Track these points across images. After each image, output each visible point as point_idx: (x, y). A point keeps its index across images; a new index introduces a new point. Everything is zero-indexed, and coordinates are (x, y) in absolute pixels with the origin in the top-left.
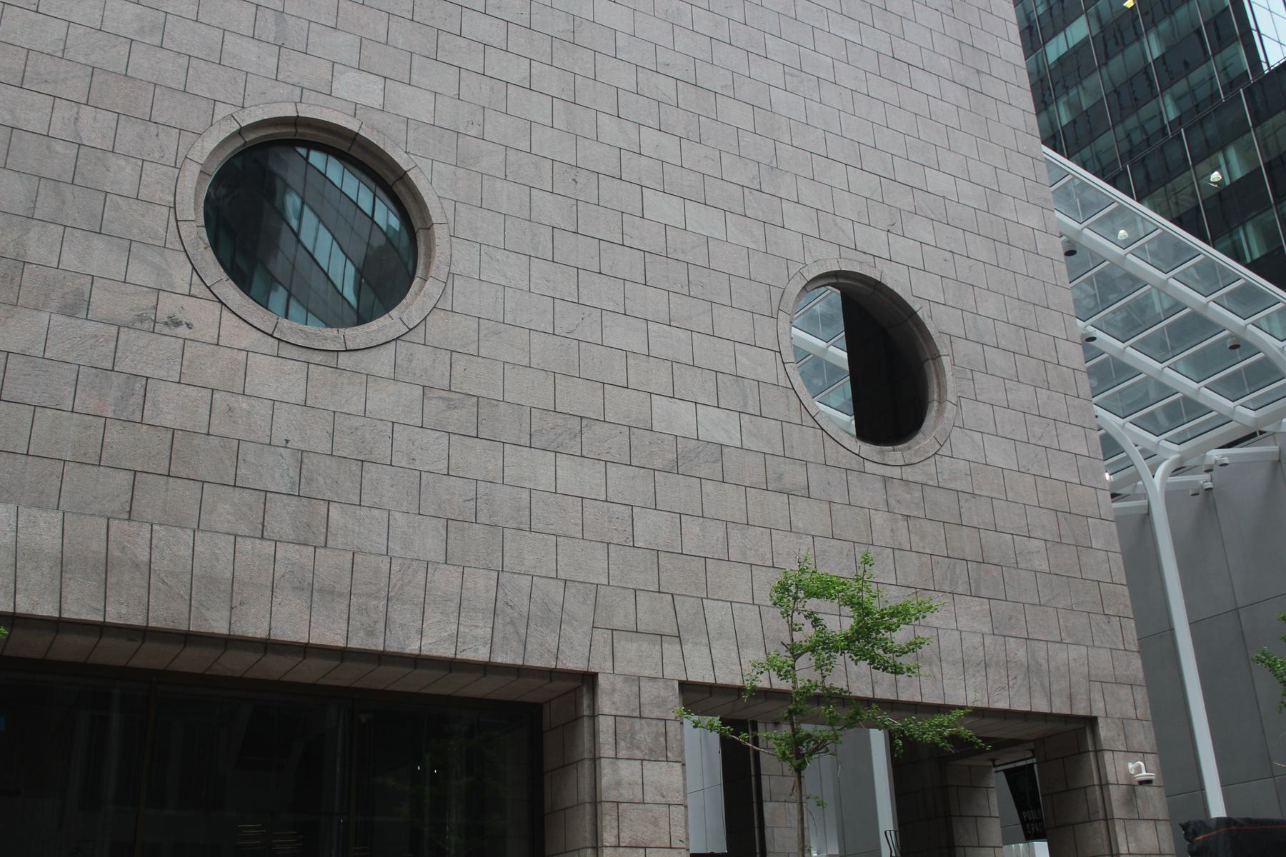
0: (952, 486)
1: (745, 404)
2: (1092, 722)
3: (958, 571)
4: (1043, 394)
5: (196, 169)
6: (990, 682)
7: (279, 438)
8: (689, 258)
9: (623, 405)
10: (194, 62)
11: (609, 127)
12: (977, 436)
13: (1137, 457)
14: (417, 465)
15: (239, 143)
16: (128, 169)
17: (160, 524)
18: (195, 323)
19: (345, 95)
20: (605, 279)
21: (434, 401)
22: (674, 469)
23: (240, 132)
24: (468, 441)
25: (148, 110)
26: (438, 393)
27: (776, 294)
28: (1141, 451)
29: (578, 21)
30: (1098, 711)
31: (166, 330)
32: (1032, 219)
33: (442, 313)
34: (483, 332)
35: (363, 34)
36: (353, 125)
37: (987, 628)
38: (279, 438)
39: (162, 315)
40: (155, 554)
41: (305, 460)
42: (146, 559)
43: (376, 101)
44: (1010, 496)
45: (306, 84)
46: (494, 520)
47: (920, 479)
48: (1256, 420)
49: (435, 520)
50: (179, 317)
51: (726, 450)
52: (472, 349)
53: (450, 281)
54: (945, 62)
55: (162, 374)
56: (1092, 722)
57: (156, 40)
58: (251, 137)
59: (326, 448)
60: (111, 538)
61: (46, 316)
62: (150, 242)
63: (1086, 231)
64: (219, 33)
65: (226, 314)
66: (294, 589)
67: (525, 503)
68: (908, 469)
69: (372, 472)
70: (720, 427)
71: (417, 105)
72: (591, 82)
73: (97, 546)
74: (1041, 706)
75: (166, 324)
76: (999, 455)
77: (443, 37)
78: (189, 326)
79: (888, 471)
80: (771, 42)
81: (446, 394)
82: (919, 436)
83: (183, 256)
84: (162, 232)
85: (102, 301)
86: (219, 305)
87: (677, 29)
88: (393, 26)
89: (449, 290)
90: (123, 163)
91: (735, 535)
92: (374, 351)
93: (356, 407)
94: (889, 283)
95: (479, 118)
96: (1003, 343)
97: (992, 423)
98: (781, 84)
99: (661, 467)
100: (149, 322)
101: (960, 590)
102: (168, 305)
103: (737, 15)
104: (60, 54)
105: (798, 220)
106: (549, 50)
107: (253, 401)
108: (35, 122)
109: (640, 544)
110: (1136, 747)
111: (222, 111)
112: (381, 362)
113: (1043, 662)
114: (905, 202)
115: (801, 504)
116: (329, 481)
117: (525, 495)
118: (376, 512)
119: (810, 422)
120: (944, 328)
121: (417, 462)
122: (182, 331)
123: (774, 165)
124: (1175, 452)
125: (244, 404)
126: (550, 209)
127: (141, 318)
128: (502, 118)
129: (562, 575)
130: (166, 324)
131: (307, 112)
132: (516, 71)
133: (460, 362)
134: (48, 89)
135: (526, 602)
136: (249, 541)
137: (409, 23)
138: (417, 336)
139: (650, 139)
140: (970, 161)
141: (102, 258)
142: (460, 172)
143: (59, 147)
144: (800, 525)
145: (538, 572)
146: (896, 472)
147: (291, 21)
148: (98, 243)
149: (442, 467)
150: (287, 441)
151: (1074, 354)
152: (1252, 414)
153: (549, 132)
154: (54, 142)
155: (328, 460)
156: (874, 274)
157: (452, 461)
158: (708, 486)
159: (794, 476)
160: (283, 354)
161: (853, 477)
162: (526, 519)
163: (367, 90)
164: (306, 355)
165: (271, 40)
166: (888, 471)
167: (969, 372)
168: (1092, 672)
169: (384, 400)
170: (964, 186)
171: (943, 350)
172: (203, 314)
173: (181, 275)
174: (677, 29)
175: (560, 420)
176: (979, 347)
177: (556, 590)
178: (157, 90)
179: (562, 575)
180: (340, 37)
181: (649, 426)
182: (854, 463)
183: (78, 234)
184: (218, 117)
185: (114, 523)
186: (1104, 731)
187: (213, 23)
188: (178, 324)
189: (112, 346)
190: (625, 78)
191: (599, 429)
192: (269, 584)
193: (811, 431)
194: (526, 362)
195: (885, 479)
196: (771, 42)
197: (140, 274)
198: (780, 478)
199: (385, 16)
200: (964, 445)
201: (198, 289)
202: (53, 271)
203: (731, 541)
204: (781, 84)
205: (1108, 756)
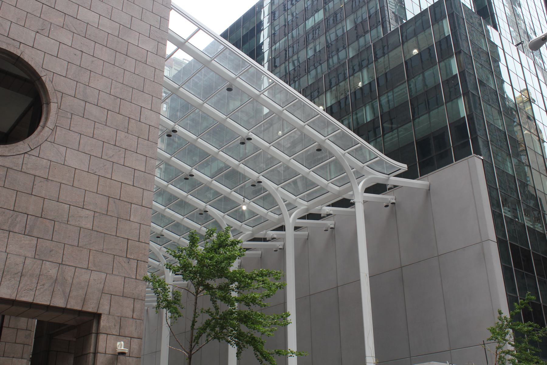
0: (32, 172)
2: (97, 316)
3: (18, 219)
4: (121, 135)
6: (21, 285)
12: (63, 149)
13: (282, 205)
28: (287, 205)
30: (104, 309)
37: (30, 254)
48: (339, 192)
56: (97, 316)
74: (59, 302)
94: (26, 58)
97: (77, 144)
101: (16, 230)
110: (127, 333)
113: (70, 280)
114: (59, 20)
124: (305, 205)
152: (337, 188)
156: (18, 52)
167: (69, 114)
168: (106, 288)
170: (105, 21)
171: (53, 98)
176: (83, 103)
186: (104, 322)
200: (49, 152)
205: (102, 337)
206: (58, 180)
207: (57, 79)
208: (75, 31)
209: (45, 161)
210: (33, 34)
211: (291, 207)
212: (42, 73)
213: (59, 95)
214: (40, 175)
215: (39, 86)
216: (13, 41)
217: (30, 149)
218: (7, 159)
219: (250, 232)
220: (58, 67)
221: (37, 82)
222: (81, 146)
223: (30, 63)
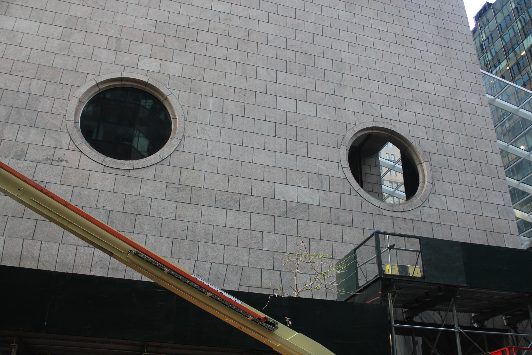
1: (322, 186)
4: (479, 177)
5: (77, 100)
7: (100, 205)
9: (260, 188)
10: (80, 59)
11: (262, 72)
12: (443, 198)
14: (161, 216)
15: (97, 89)
16: (49, 102)
17: (45, 241)
18: (68, 160)
19: (143, 68)
20: (256, 135)
21: (171, 189)
22: (285, 215)
23: (97, 85)
24: (185, 205)
25: (59, 79)
26: (173, 185)
27: (340, 138)
29: (250, 31)
31: (57, 164)
32: (475, 100)
33: (178, 152)
34: (197, 159)
35: (153, 44)
36: (145, 79)
38: (100, 205)
39: (56, 158)
40: (42, 254)
41: (111, 214)
42: (37, 255)
43: (157, 69)
44: (460, 224)
45: (126, 64)
46: (195, 238)
47: (412, 217)
49: (167, 239)
50: (63, 158)
51: (311, 207)
52: (191, 167)
53: (183, 139)
54: (430, 36)
55: (53, 180)
57: (66, 53)
58: (102, 87)
59: (121, 209)
60: (24, 247)
61: (8, 159)
62: (54, 129)
63: (521, 110)
64: (92, 48)
65: (83, 156)
66: (101, 268)
67: (211, 231)
68: (406, 213)
69: (140, 219)
70: (308, 196)
71: (174, 69)
72: (255, 55)
73: (18, 250)
75: (57, 161)
76: (454, 206)
77: (188, 42)
78: (67, 161)
79: (394, 214)
80: (342, 34)
81: (177, 186)
82: (414, 198)
83: (67, 134)
84: (59, 125)
85: (31, 153)
86: (80, 153)
87: (297, 31)
88: (167, 39)
89: (182, 143)
90: (47, 100)
91: (314, 245)
92: (146, 169)
93: (136, 192)
95: (202, 72)
96: (458, 155)
97: (451, 191)
98: (347, 50)
99: (278, 215)
100: (50, 161)
102: (59, 154)
103: (327, 23)
104: (26, 61)
105: (353, 106)
106: (236, 44)
107: (90, 191)
108: (13, 86)
109: (266, 249)
111: (90, 77)
112: (149, 174)
114: (408, 95)
115: (348, 230)
116: (120, 223)
117: (211, 228)
118: (141, 236)
120: (426, 150)
121: (162, 214)
122: (64, 163)
123: (342, 83)
125: (86, 192)
126: (231, 107)
127: (47, 159)
128: (213, 73)
129: (226, 262)
130: (57, 161)
131: (125, 75)
132: (221, 53)
133: (185, 172)
134: (20, 74)
135: (208, 274)
136: (82, 248)
137: (174, 38)
138: (166, 162)
140: (442, 77)
141: (33, 136)
142: (192, 95)
143: (22, 95)
144: (348, 239)
145: (215, 261)
146: (399, 215)
147: (123, 41)
148: (33, 131)
149: (173, 216)
150: (104, 207)
151: (497, 160)
153: (234, 76)
154: (20, 94)
155: (121, 214)
156: (391, 127)
157: (178, 214)
158: (301, 223)
159: (346, 217)
160: (106, 171)
161: (376, 217)
162: (210, 238)
163: (154, 65)
164: (115, 171)
165: (114, 49)
166: (394, 214)
169: (148, 189)
170: (438, 88)
172: (73, 157)
173: (66, 141)
175: (230, 195)
177: (222, 269)
178: (64, 71)
179: (226, 262)
180: (143, 45)
182: (377, 211)
183: (25, 128)
184: (88, 80)
185: (26, 241)
187: (90, 44)
188: (62, 161)
189: (34, 170)
190: (272, 53)
191: (248, 199)
192: (90, 266)
193: (355, 197)
194: (215, 171)
195: (393, 218)
196: (342, 34)
197: (49, 142)
198: (338, 218)
199: (164, 36)
200: (436, 202)
201: (72, 147)
202: (13, 143)
203: (311, 247)
204: (347, 50)
207: (422, 142)
208: (422, 101)
209: (435, 209)
210: (396, 111)
212: (411, 140)
213: (428, 154)
214: (435, 221)
215: (412, 151)
216: (386, 120)
218: (410, 213)
219: (528, 243)
220: (420, 132)
221: (409, 148)
222: (455, 193)
223: (401, 134)
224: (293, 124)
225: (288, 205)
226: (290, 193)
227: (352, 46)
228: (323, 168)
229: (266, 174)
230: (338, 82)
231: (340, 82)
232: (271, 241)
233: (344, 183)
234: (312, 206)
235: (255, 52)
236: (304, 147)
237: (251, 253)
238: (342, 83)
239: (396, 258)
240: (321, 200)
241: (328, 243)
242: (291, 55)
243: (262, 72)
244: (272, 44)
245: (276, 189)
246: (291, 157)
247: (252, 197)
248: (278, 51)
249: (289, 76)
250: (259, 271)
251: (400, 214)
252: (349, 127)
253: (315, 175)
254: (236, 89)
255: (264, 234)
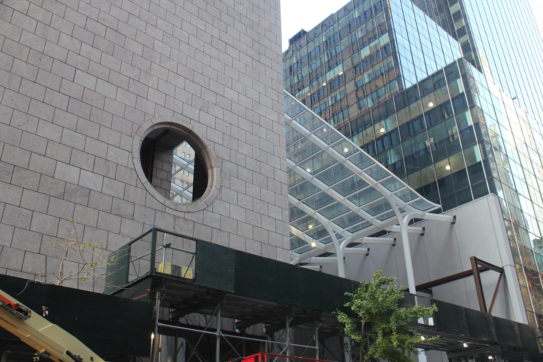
0: (210, 225)
4: (264, 191)
8: (94, 104)
11: (65, 40)
12: (227, 205)
13: (333, 236)
20: (45, 105)
22: (62, 197)
27: (136, 127)
28: (336, 235)
32: (273, 117)
44: (239, 233)
47: (194, 219)
48: (382, 225)
51: (92, 192)
54: (245, 47)
63: (313, 135)
70: (90, 180)
76: (237, 214)
80: (160, 21)
82: (199, 200)
87: (113, 6)
91: (88, 231)
94: (196, 131)
96: (248, 166)
98: (161, 39)
99: (54, 195)
103: (146, 6)
109: (34, 230)
119: (140, 185)
120: (220, 155)
123: (149, 72)
124: (350, 236)
139: (86, 49)
140: (248, 88)
144: (125, 232)
151: (283, 177)
152: (380, 222)
153: (32, 35)
156: (189, 127)
158: (79, 208)
159: (127, 209)
161: (158, 214)
170: (242, 97)
174: (113, 6)
181: (52, 175)
182: (160, 207)
193: (140, 190)
195: (175, 217)
196: (160, 21)
198: (119, 209)
203: (85, 234)
204: (161, 39)
206: (227, 230)
207: (217, 147)
208: (224, 107)
211: (339, 237)
212: (207, 143)
215: (205, 153)
217: (206, 206)
219: (298, 258)
220: (217, 137)
221: (203, 150)
222: (239, 202)
223: (198, 135)
224: (89, 102)
225: (67, 187)
226: (72, 174)
227: (167, 37)
228: (112, 154)
229: (48, 149)
230: (145, 70)
231: (147, 70)
232: (40, 222)
233: (131, 173)
234: (94, 192)
235: (62, 15)
236: (95, 129)
237: (16, 232)
238: (149, 72)
239: (171, 258)
240: (104, 186)
241: (103, 233)
242: (101, 29)
243: (65, 40)
244: (82, 12)
245: (57, 167)
246: (80, 136)
247: (28, 171)
248: (88, 21)
249: (94, 50)
250: (22, 253)
251: (183, 214)
252: (147, 118)
253: (102, 160)
254: (32, 50)
255: (35, 213)
